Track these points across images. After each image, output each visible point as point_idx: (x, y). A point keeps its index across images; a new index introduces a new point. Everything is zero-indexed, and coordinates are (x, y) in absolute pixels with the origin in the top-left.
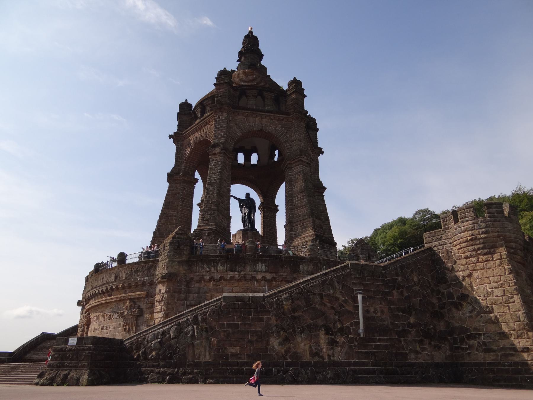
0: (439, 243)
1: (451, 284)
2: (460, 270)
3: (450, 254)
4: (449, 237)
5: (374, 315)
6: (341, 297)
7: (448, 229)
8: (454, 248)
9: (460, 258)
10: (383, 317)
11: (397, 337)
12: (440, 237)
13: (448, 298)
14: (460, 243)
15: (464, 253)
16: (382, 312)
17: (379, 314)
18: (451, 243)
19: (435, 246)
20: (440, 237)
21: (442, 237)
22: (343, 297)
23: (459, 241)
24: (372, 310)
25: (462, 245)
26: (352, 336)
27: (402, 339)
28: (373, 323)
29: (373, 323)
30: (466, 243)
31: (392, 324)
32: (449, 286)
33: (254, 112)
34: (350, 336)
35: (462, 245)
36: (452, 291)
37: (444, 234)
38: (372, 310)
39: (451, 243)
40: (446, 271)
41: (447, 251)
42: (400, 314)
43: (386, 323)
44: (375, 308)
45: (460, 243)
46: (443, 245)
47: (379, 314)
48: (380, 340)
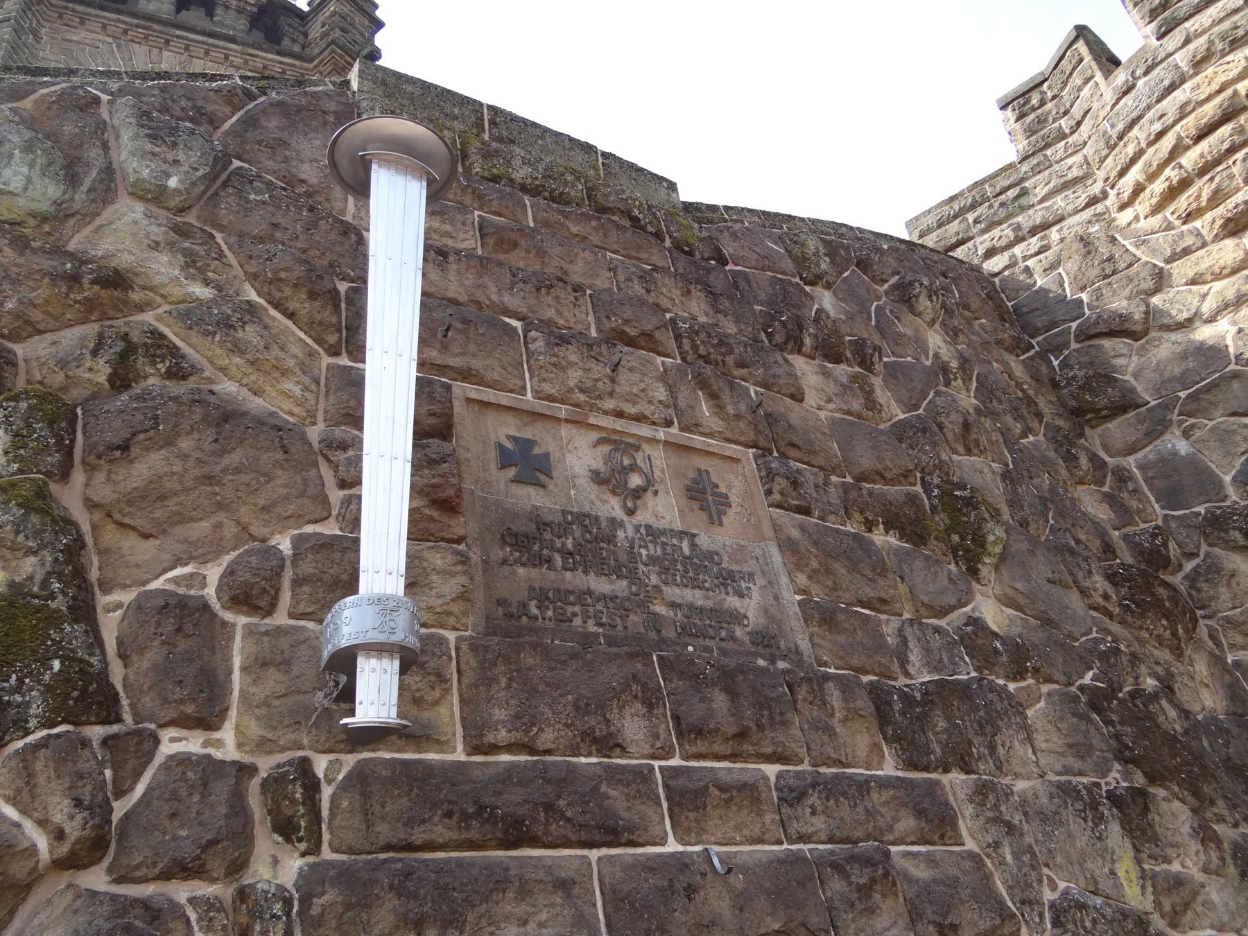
0: (1018, 227)
1: (1167, 407)
2: (1207, 307)
3: (1104, 250)
4: (1075, 172)
5: (613, 507)
6: (164, 268)
7: (1063, 136)
8: (1126, 216)
9: (1189, 241)
10: (718, 539)
11: (889, 768)
12: (1011, 193)
13: (1171, 498)
14: (1177, 150)
15: (1217, 198)
16: (702, 495)
17: (664, 509)
18: (1093, 201)
19: (990, 253)
20: (1011, 193)
21: (1024, 193)
22: (193, 266)
23: (1168, 142)
24: (578, 456)
25: (1190, 159)
26: (227, 744)
27: (955, 782)
28: (602, 585)
29: (602, 585)
30: (1225, 130)
32: (1157, 426)
33: (156, 27)
34: (174, 743)
35: (1190, 159)
36: (1183, 447)
37: (1036, 171)
38: (578, 456)
39: (1093, 201)
40: (1106, 343)
41: (1085, 241)
42: (883, 539)
43: (751, 607)
45: (1177, 150)
46: (1046, 226)
47: (664, 509)
48: (689, 800)
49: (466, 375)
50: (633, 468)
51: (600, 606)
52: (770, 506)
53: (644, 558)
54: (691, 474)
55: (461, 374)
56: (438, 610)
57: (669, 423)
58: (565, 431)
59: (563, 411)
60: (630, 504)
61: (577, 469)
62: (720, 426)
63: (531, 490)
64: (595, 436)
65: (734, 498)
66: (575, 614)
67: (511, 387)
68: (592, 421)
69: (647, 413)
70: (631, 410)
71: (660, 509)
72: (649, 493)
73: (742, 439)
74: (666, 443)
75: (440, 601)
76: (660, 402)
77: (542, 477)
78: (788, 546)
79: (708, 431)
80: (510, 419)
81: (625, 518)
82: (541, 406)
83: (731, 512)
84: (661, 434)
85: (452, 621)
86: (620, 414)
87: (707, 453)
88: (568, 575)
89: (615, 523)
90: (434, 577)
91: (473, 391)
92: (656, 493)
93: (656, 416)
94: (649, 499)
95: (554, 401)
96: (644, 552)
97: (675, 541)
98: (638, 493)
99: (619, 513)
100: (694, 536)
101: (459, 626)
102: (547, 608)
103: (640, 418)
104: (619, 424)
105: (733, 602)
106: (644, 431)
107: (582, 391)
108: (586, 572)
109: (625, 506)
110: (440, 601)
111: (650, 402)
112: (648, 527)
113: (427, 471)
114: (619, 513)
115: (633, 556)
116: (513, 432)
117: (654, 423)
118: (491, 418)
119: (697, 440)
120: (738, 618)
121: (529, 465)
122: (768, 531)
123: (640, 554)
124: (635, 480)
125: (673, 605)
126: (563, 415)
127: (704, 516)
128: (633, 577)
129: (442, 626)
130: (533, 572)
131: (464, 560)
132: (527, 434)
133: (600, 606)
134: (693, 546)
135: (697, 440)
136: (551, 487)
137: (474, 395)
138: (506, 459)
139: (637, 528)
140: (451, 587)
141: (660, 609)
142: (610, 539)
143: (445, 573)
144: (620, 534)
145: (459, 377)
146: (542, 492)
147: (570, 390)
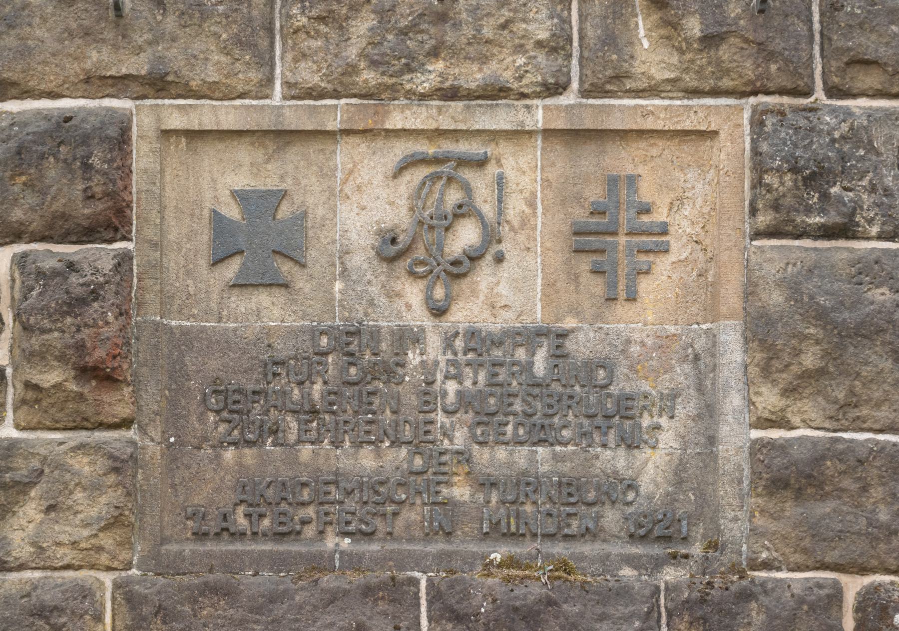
16: (606, 241)
17: (511, 293)
24: (361, 197)
31: (786, 478)
44: (443, 164)
49: (158, 84)
50: (463, 211)
51: (351, 504)
52: (758, 234)
53: (451, 398)
54: (595, 193)
55: (152, 84)
56: (83, 545)
57: (555, 88)
58: (344, 154)
59: (336, 113)
60: (439, 293)
61: (353, 236)
62: (669, 67)
63: (263, 298)
64: (401, 149)
65: (683, 225)
66: (305, 522)
67: (240, 88)
68: (396, 120)
69: (507, 76)
70: (473, 76)
71: (503, 289)
72: (489, 258)
73: (726, 83)
74: (548, 133)
75: (86, 533)
76: (540, 44)
77: (286, 267)
78: (760, 330)
79: (643, 84)
80: (244, 153)
81: (428, 322)
82: (296, 115)
83: (663, 265)
84: (538, 115)
85: (104, 559)
86: (451, 94)
87: (641, 133)
88: (306, 451)
89: (408, 338)
90: (79, 495)
91: (176, 114)
92: (499, 259)
93: (528, 79)
94: (484, 276)
95: (322, 96)
96: (452, 387)
97: (521, 354)
98: (460, 269)
99: (416, 315)
100: (563, 335)
101: (116, 564)
102: (262, 516)
103: (495, 93)
104: (452, 115)
105: (613, 459)
106: (500, 118)
107: (374, 64)
108: (336, 444)
109: (428, 299)
110: (86, 533)
111: (520, 49)
112: (472, 334)
113: (69, 320)
114: (416, 315)
115: (428, 397)
116: (243, 181)
117: (524, 96)
118: (209, 157)
119: (622, 111)
120: (617, 489)
121: (261, 242)
122: (731, 295)
123: (445, 394)
124: (466, 235)
125: (487, 484)
126: (333, 124)
127: (597, 286)
128: (421, 442)
129: (92, 567)
130: (249, 455)
131: (121, 465)
132: (270, 182)
133: (351, 504)
134: (558, 355)
135: (622, 111)
136: (300, 284)
137: (176, 122)
138: (225, 244)
139: (448, 343)
140: (99, 507)
141: (461, 491)
142: (390, 371)
143: (94, 488)
144: (413, 358)
145: (149, 90)
146: (280, 295)
147: (352, 70)
